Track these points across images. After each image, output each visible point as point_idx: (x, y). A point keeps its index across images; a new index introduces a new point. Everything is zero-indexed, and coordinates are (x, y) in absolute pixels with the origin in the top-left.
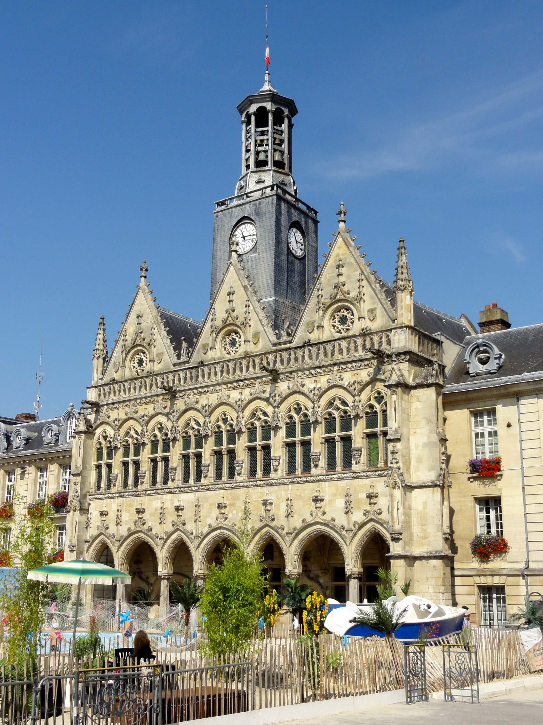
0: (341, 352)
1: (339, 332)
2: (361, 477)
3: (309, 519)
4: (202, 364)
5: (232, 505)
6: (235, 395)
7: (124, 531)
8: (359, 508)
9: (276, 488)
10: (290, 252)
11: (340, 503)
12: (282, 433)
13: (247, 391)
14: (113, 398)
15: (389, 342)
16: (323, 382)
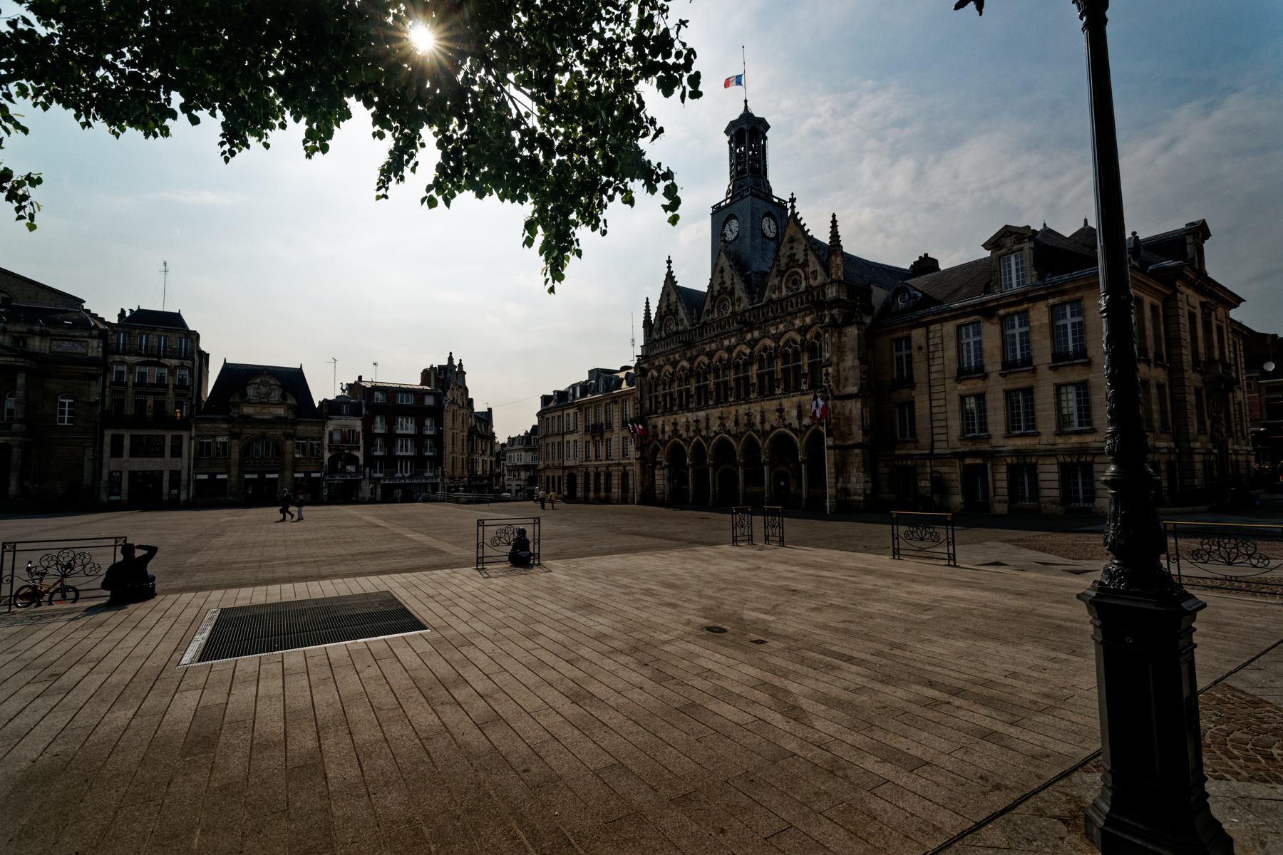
0: (792, 307)
1: (792, 291)
2: (807, 394)
3: (775, 424)
4: (705, 323)
5: (728, 417)
6: (726, 343)
7: (666, 437)
8: (806, 416)
9: (753, 405)
10: (764, 236)
11: (794, 413)
14: (655, 352)
15: (824, 295)
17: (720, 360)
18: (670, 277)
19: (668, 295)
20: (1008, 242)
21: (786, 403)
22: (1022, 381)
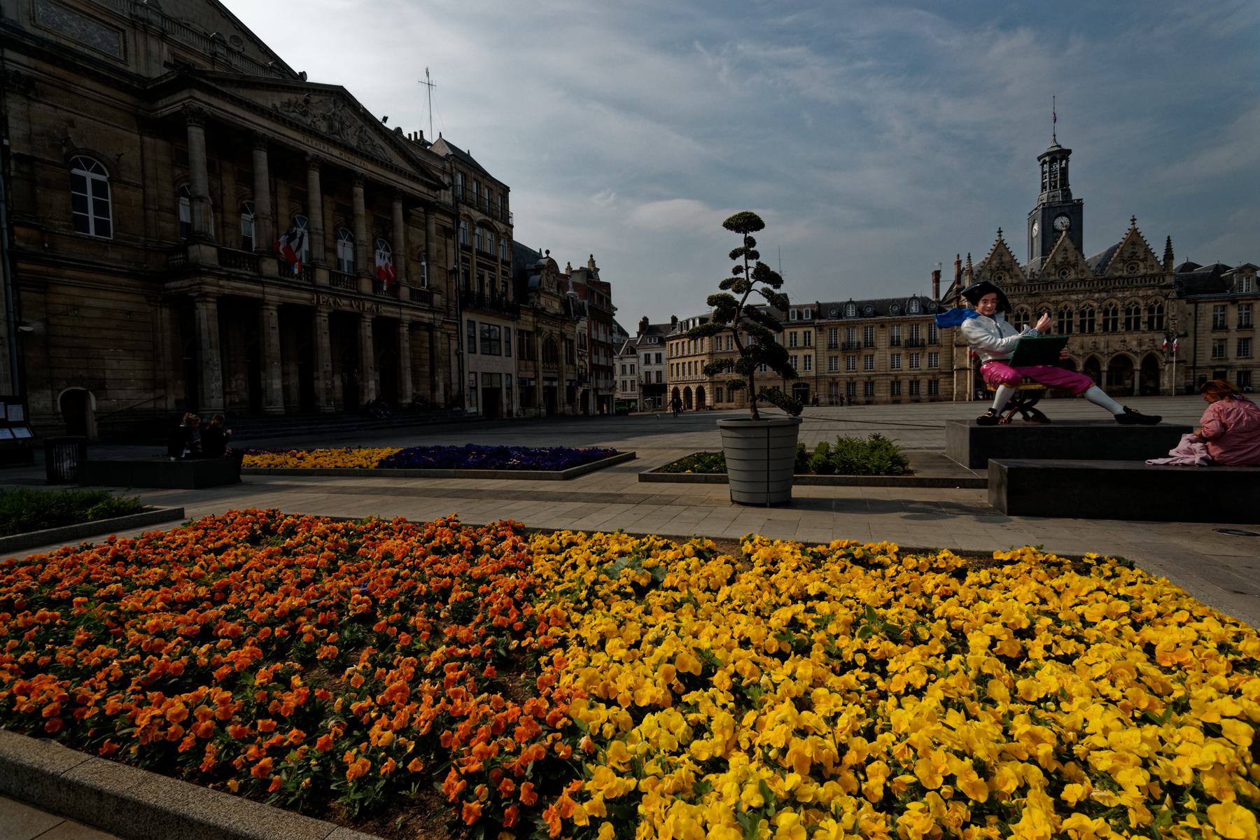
6: (1074, 297)
11: (1135, 343)
12: (1102, 315)
13: (1081, 296)
16: (1127, 293)
17: (1066, 307)
18: (1001, 244)
19: (1001, 255)
20: (1247, 271)
21: (1128, 338)
22: (1246, 334)
